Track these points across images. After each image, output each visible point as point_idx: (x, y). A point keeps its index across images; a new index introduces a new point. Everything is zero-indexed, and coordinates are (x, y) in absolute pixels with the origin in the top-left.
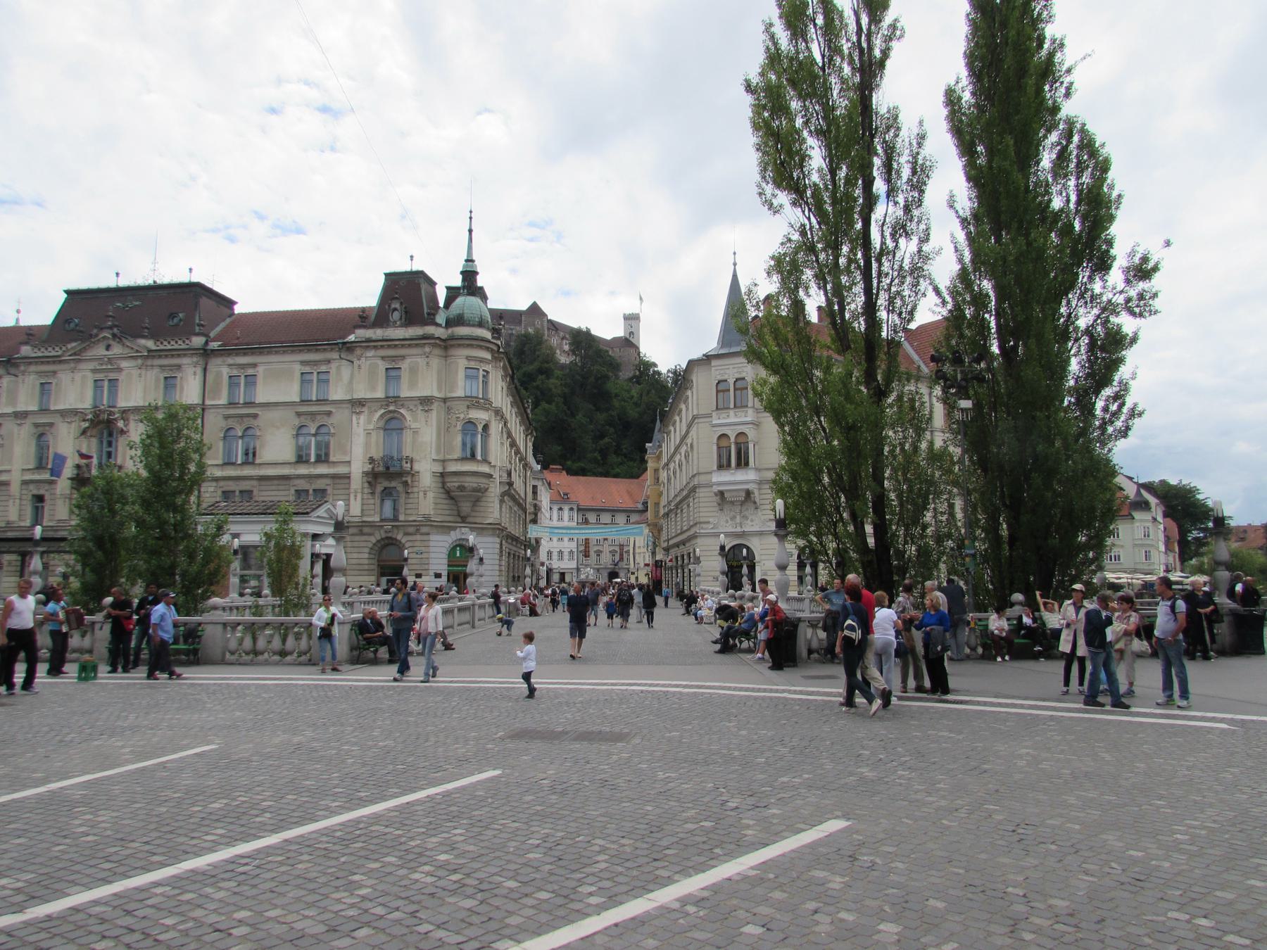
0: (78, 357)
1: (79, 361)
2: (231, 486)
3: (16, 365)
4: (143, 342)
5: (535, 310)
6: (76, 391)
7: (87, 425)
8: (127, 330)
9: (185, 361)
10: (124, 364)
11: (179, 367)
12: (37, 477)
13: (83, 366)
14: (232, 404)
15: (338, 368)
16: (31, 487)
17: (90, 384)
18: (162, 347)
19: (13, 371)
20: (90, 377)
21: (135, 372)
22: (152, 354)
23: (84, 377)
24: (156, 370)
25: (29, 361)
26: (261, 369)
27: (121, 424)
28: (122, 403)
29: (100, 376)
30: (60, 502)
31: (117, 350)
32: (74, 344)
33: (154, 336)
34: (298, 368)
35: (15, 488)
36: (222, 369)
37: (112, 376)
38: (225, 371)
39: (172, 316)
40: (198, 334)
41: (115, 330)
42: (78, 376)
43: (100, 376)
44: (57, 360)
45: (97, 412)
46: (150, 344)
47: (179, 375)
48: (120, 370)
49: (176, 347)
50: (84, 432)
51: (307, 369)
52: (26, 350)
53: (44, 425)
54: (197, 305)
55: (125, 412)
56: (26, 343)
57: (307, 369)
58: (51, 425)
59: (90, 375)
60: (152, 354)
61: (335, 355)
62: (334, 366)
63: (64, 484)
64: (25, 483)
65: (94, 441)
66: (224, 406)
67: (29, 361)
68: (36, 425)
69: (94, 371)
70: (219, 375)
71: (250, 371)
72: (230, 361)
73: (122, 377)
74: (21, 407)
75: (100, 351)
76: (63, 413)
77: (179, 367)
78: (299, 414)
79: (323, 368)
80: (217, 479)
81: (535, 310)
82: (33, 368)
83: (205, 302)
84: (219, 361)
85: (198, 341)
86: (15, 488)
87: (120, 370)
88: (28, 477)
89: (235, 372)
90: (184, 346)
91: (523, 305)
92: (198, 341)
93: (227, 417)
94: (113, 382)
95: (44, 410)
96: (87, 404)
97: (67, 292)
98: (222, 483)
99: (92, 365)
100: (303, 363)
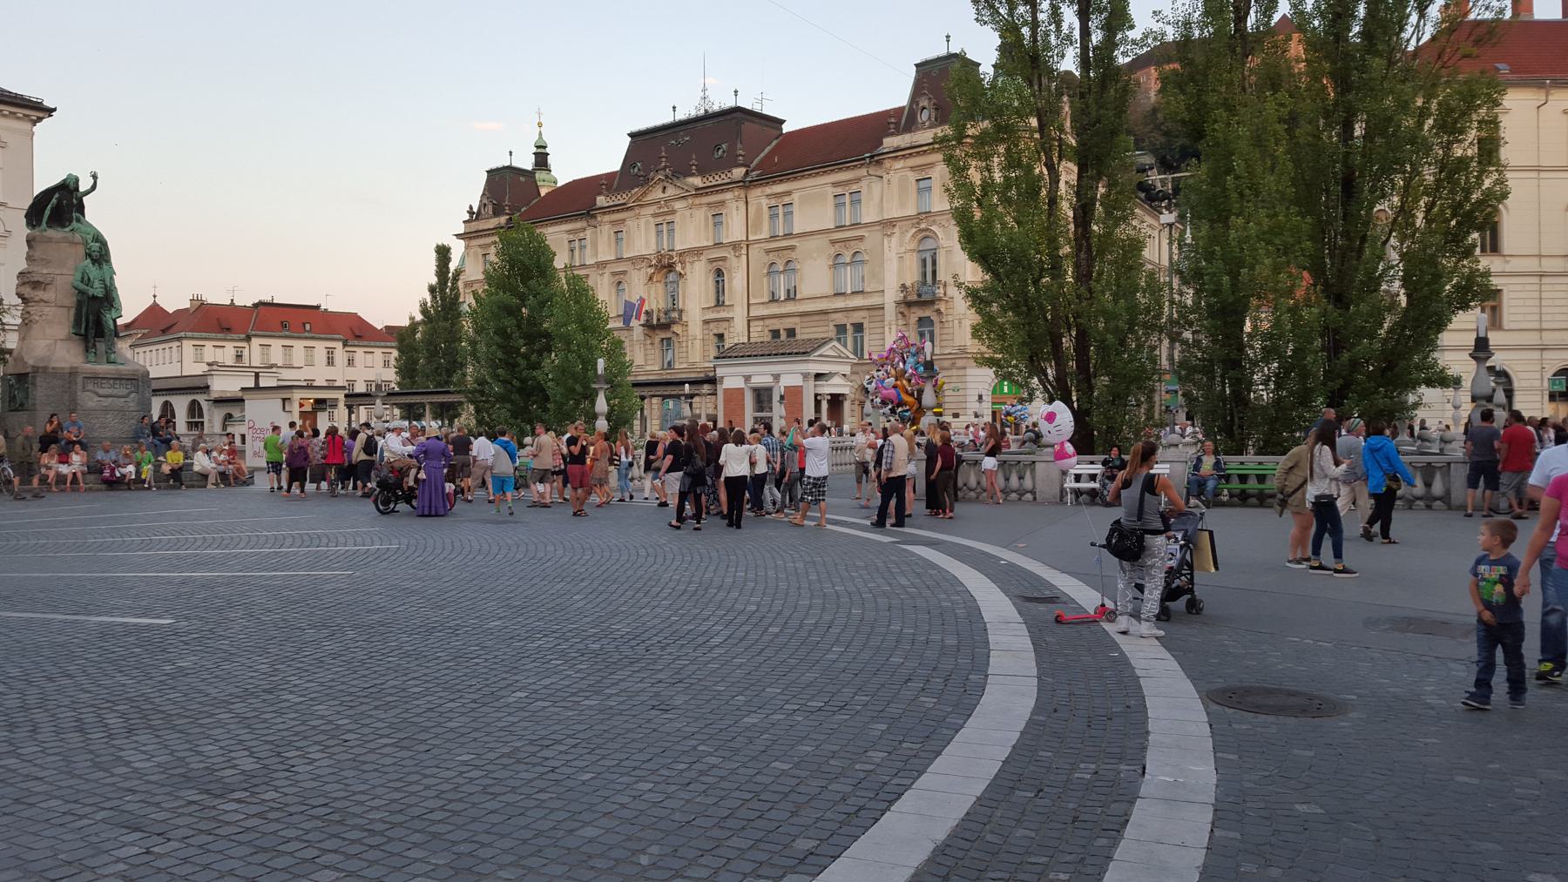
3: (594, 217)
4: (691, 180)
6: (642, 238)
8: (680, 172)
9: (728, 196)
10: (678, 205)
11: (723, 203)
15: (869, 186)
17: (653, 230)
19: (592, 222)
21: (688, 213)
22: (700, 192)
23: (647, 222)
24: (704, 209)
26: (795, 197)
27: (679, 268)
29: (659, 220)
30: (637, 348)
31: (671, 191)
33: (702, 172)
34: (831, 191)
36: (760, 198)
38: (765, 202)
42: (643, 221)
44: (623, 208)
46: (697, 181)
51: (839, 191)
56: (600, 194)
57: (839, 191)
58: (624, 273)
59: (652, 220)
61: (863, 172)
62: (864, 183)
65: (660, 286)
66: (766, 241)
68: (614, 274)
69: (655, 215)
70: (759, 210)
71: (787, 200)
72: (768, 190)
73: (677, 218)
74: (602, 257)
75: (657, 194)
78: (833, 242)
79: (854, 188)
80: (762, 318)
82: (607, 218)
83: (747, 126)
84: (758, 192)
85: (738, 173)
87: (673, 212)
93: (768, 252)
97: (631, 135)
98: (768, 322)
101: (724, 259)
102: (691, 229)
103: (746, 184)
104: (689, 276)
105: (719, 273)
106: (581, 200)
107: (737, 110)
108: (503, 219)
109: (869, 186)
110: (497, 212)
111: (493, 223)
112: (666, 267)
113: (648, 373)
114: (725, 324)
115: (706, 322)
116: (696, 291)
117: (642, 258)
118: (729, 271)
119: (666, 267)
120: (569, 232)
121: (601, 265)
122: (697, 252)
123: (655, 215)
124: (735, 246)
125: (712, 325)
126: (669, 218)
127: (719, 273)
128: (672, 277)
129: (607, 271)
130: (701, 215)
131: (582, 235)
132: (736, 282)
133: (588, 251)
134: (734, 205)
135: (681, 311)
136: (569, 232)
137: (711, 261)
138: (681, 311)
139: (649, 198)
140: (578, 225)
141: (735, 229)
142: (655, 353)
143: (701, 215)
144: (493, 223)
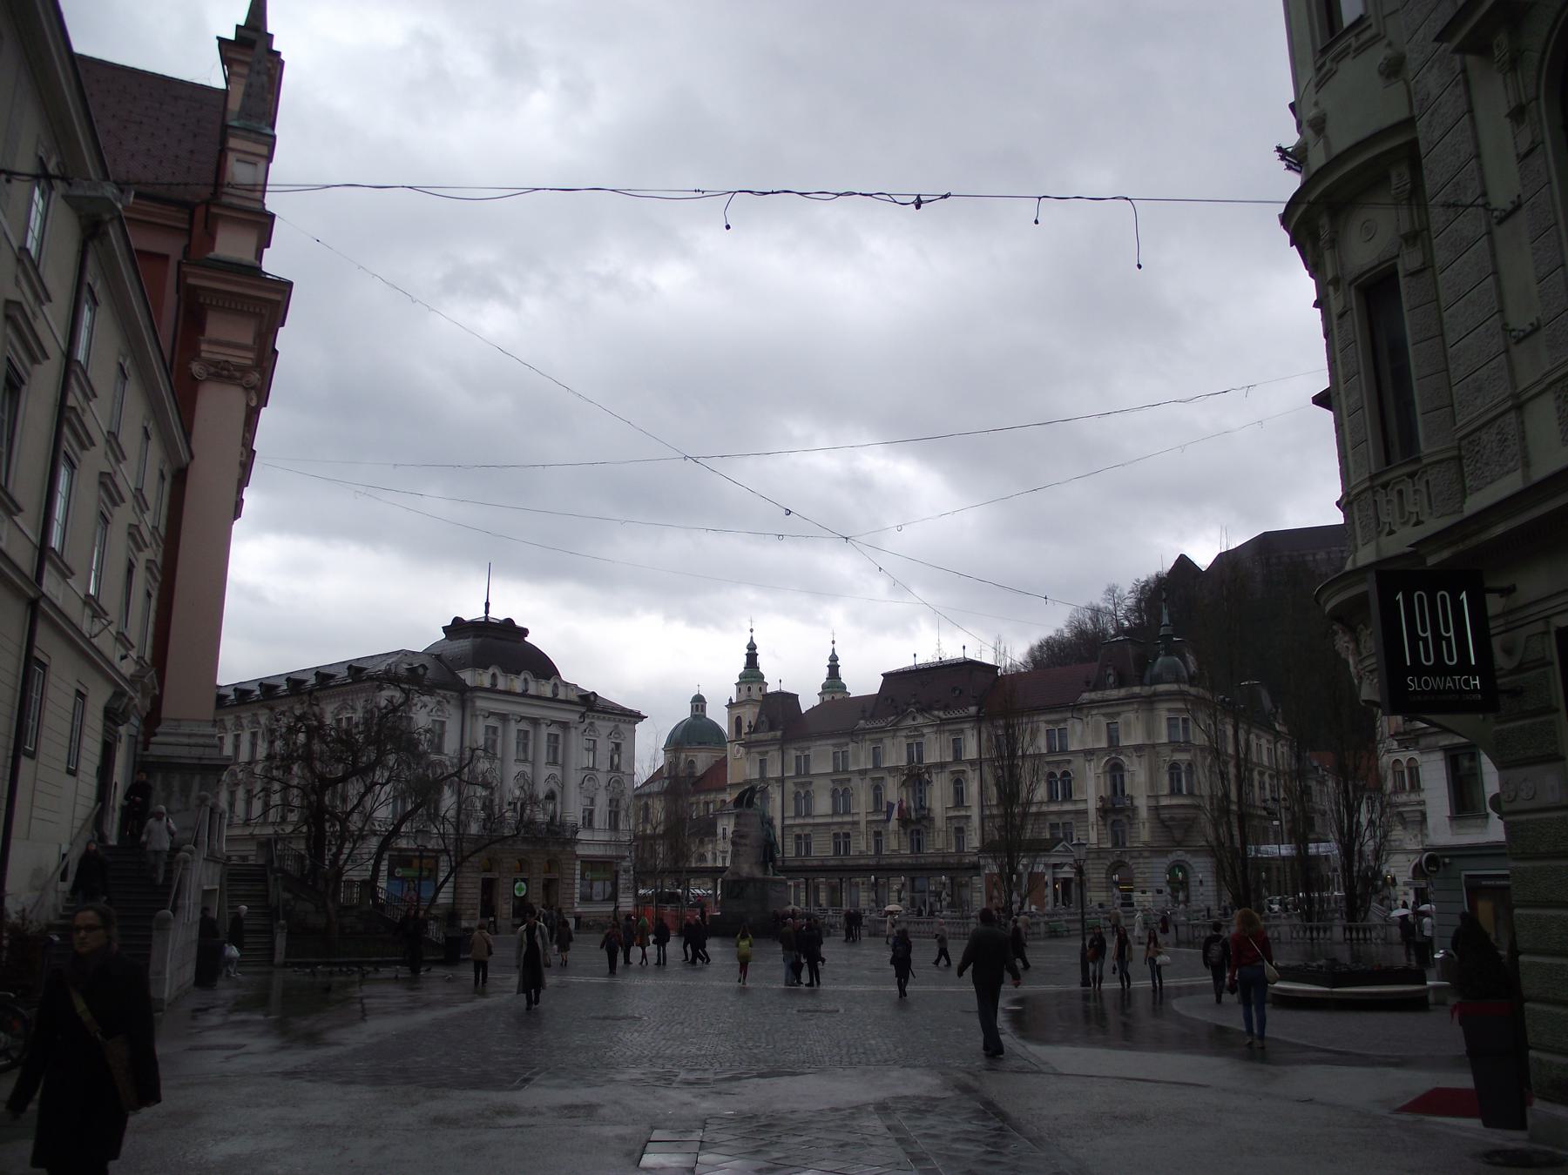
0: (896, 729)
1: (895, 731)
9: (966, 726)
10: (925, 731)
17: (905, 747)
21: (933, 737)
22: (943, 722)
25: (865, 731)
28: (928, 760)
31: (920, 720)
33: (946, 708)
35: (863, 825)
44: (882, 730)
46: (941, 714)
48: (923, 735)
55: (929, 767)
60: (943, 722)
63: (894, 824)
67: (865, 731)
68: (873, 779)
69: (907, 737)
75: (910, 722)
76: (890, 770)
77: (962, 731)
79: (1062, 726)
86: (863, 825)
87: (923, 735)
88: (871, 818)
94: (920, 745)
95: (877, 767)
96: (904, 763)
99: (904, 733)
100: (1048, 722)
108: (779, 733)
110: (772, 728)
111: (770, 735)
112: (916, 778)
113: (904, 856)
115: (949, 818)
116: (939, 797)
117: (896, 769)
119: (916, 778)
120: (834, 745)
121: (863, 772)
122: (942, 766)
124: (971, 762)
129: (868, 777)
130: (947, 738)
132: (973, 789)
133: (851, 759)
137: (953, 773)
140: (842, 740)
142: (906, 842)
143: (947, 738)
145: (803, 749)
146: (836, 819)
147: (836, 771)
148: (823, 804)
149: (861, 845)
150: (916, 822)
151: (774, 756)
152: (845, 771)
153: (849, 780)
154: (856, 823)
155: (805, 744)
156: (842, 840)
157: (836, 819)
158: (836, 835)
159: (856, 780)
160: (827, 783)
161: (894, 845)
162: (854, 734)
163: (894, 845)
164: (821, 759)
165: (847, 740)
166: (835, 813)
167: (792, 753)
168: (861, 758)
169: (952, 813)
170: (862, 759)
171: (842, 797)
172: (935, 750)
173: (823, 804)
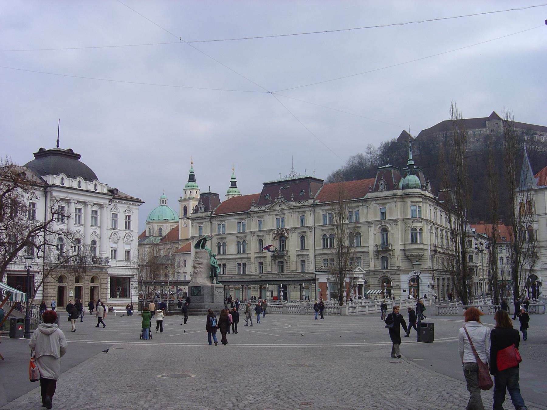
0: (270, 210)
2: (326, 257)
3: (250, 214)
4: (291, 203)
5: (494, 116)
7: (274, 235)
9: (307, 209)
10: (286, 212)
11: (305, 211)
12: (259, 255)
13: (272, 213)
14: (325, 225)
15: (362, 209)
16: (258, 259)
18: (298, 205)
19: (249, 216)
20: (275, 218)
21: (290, 215)
24: (297, 213)
28: (286, 227)
29: (278, 217)
30: (268, 265)
31: (283, 207)
32: (269, 205)
33: (296, 200)
35: (253, 260)
37: (282, 216)
38: (321, 212)
39: (301, 191)
40: (311, 199)
41: (282, 199)
42: (271, 217)
43: (278, 217)
44: (263, 211)
45: (278, 230)
46: (294, 204)
47: (305, 215)
48: (284, 214)
49: (303, 204)
50: (274, 238)
52: (253, 209)
53: (261, 236)
54: (309, 186)
58: (263, 236)
59: (274, 216)
60: (295, 208)
61: (361, 204)
62: (361, 208)
63: (269, 259)
64: (256, 258)
65: (278, 241)
69: (276, 215)
72: (323, 208)
73: (285, 217)
75: (277, 207)
77: (305, 211)
79: (357, 209)
80: (321, 255)
81: (494, 116)
82: (255, 215)
83: (312, 184)
84: (319, 208)
85: (311, 202)
86: (253, 260)
87: (284, 214)
88: (257, 255)
89: (325, 213)
90: (306, 204)
91: (487, 114)
92: (311, 202)
93: (323, 230)
94: (283, 218)
95: (260, 231)
96: (275, 228)
98: (323, 256)
99: (275, 213)
101: (305, 232)
102: (291, 221)
103: (314, 206)
104: (290, 238)
105: (303, 237)
106: (241, 207)
107: (310, 178)
108: (209, 213)
109: (362, 209)
110: (206, 210)
114: (306, 257)
115: (298, 256)
116: (293, 244)
117: (271, 231)
118: (307, 237)
119: (281, 236)
120: (238, 219)
121: (253, 233)
122: (294, 229)
123: (276, 215)
124: (310, 228)
125: (300, 257)
126: (282, 216)
127: (303, 237)
128: (283, 238)
129: (255, 235)
131: (244, 221)
132: (310, 241)
133: (246, 227)
134: (309, 213)
135: (287, 251)
136: (238, 219)
137: (300, 233)
138: (287, 251)
139: (274, 208)
140: (242, 217)
141: (309, 221)
144: (204, 214)
145: (221, 221)
146: (239, 256)
147: (239, 232)
148: (232, 249)
149: (253, 269)
150: (280, 258)
151: (206, 224)
152: (244, 232)
153: (246, 236)
154: (249, 258)
155: (221, 219)
156: (242, 266)
157: (239, 256)
158: (239, 264)
159: (249, 237)
160: (234, 238)
161: (269, 269)
162: (248, 214)
163: (269, 269)
164: (231, 225)
165: (245, 216)
166: (239, 253)
167: (216, 223)
168: (252, 225)
169: (300, 253)
170: (252, 226)
171: (242, 244)
172: (291, 221)
173: (232, 249)
